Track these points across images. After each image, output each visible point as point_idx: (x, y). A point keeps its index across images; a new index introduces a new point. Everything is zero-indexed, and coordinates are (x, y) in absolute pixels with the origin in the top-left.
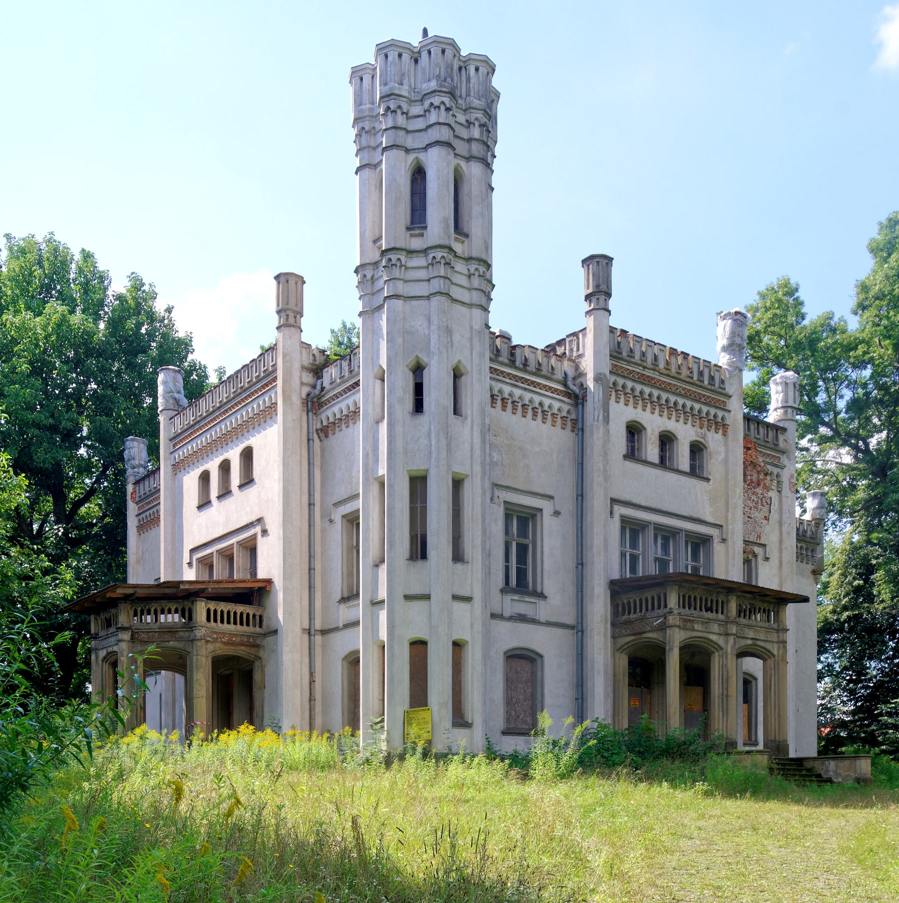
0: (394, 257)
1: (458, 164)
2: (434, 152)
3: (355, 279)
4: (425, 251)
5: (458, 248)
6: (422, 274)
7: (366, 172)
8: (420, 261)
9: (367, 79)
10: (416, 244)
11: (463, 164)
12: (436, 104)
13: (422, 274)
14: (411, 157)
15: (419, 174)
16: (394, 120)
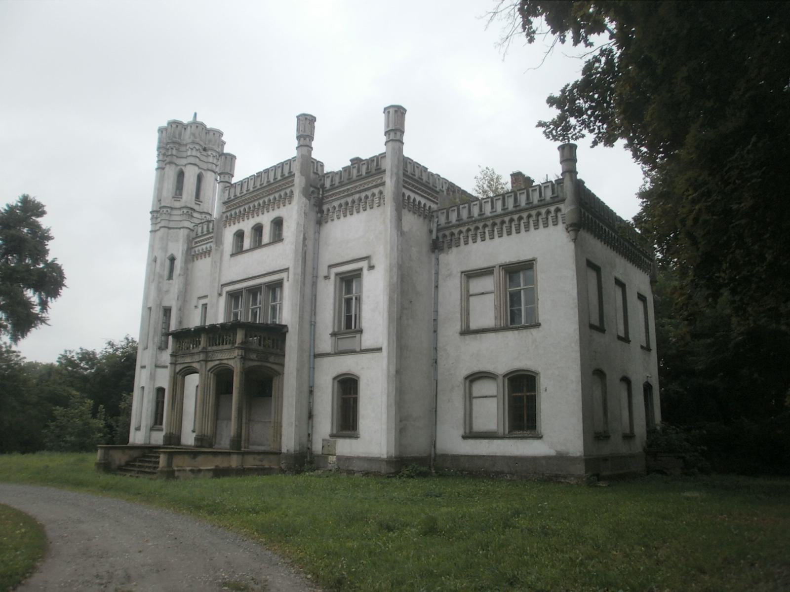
0: (165, 210)
1: (201, 172)
2: (189, 167)
3: (150, 216)
4: (180, 209)
5: (196, 208)
6: (178, 218)
7: (159, 171)
8: (179, 212)
9: (164, 132)
10: (177, 205)
11: (203, 172)
12: (192, 147)
13: (178, 218)
14: (179, 167)
15: (181, 175)
16: (172, 152)
